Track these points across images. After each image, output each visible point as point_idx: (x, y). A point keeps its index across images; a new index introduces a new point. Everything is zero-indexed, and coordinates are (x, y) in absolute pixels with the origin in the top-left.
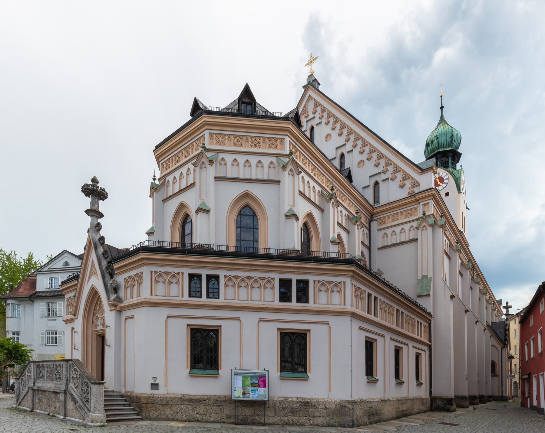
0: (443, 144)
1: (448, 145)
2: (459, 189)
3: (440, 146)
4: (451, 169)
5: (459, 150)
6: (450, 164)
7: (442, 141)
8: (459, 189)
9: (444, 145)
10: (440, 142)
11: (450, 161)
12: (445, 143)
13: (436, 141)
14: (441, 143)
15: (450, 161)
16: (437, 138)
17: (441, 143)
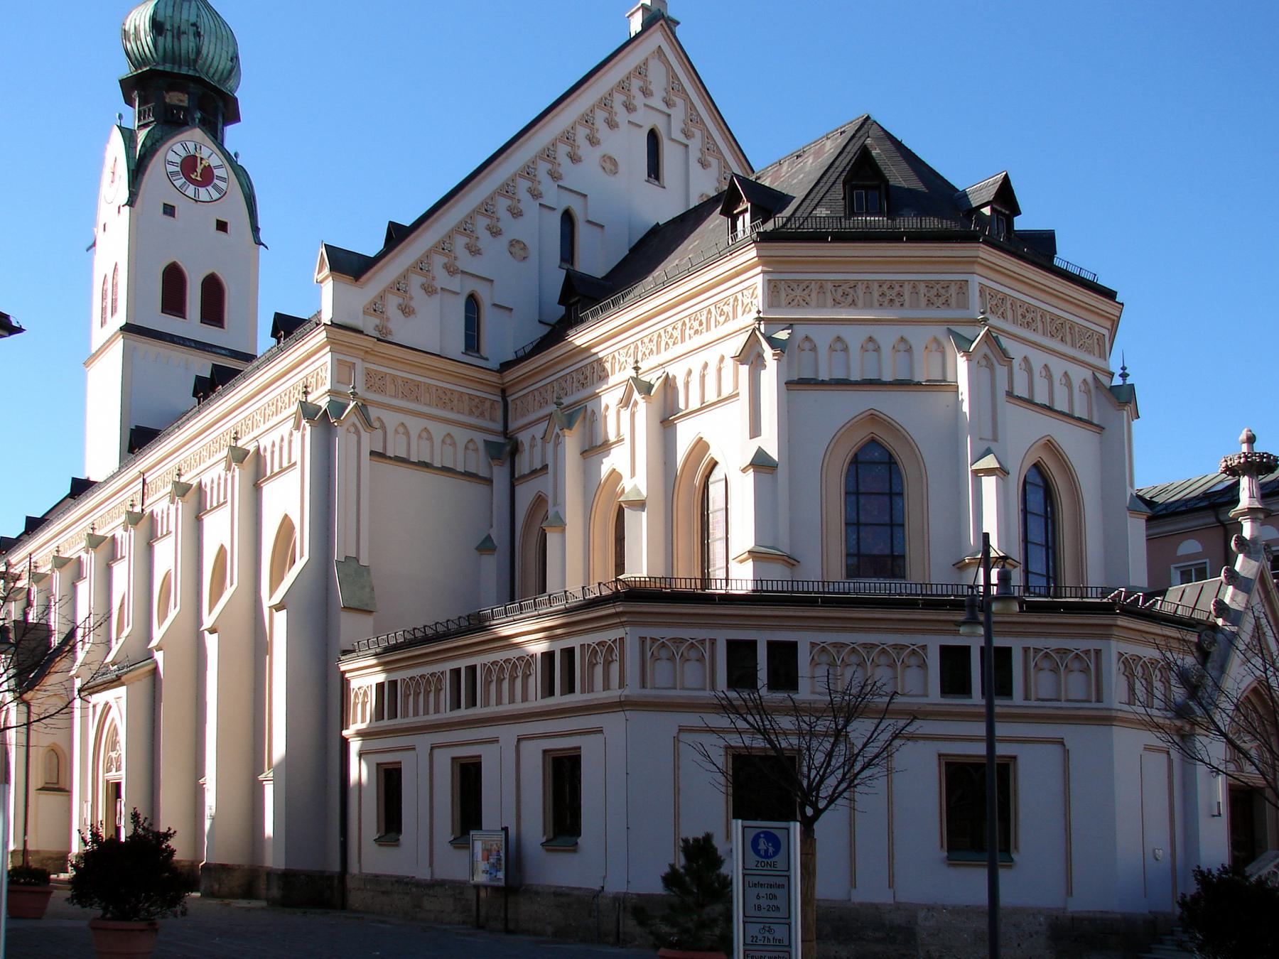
0: (210, 59)
1: (219, 74)
3: (200, 62)
7: (208, 53)
9: (210, 66)
10: (204, 52)
12: (215, 64)
13: (192, 38)
14: (205, 55)
17: (205, 55)
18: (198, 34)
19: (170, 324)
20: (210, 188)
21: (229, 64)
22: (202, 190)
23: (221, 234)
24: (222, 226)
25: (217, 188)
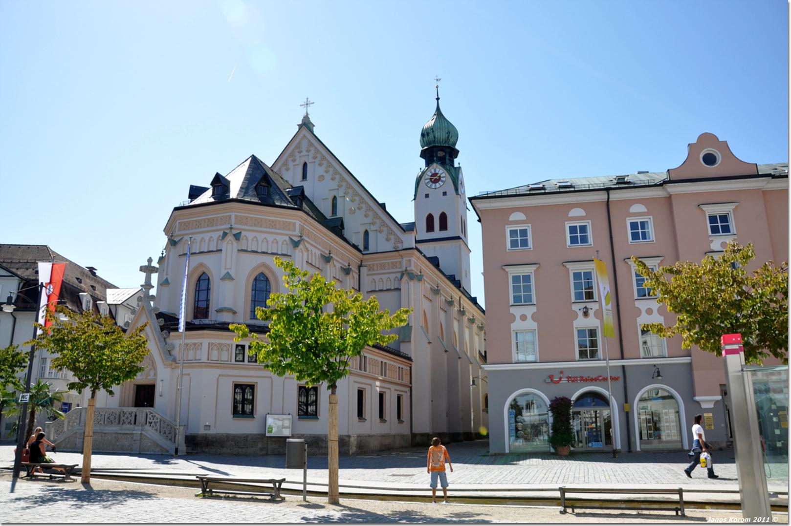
2: (457, 190)
4: (448, 167)
5: (457, 147)
6: (447, 161)
8: (457, 190)
10: (436, 136)
11: (447, 157)
15: (447, 157)
16: (433, 131)
18: (433, 131)
19: (431, 235)
20: (440, 182)
21: (447, 135)
22: (437, 184)
23: (445, 197)
24: (445, 194)
25: (442, 181)
